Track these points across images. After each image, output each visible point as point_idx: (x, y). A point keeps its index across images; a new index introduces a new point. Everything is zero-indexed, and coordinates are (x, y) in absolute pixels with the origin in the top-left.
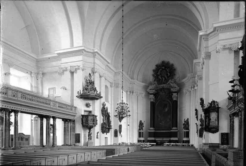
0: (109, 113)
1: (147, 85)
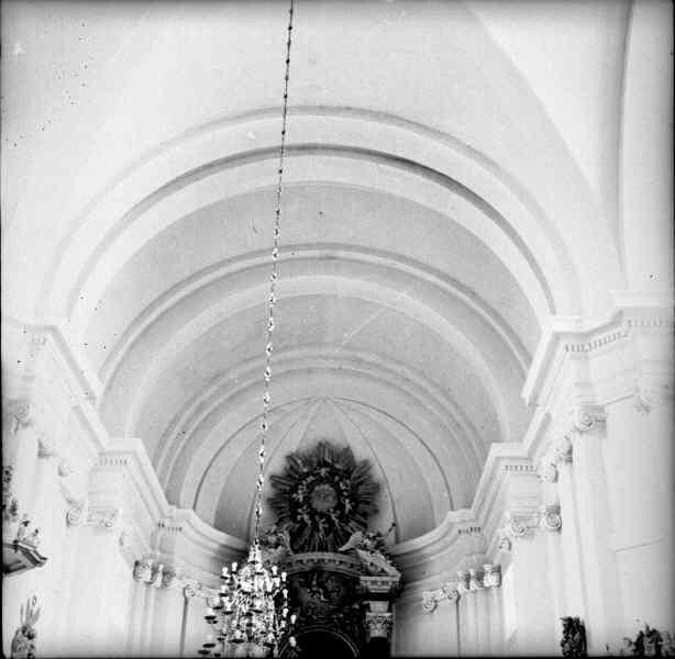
1: (237, 543)
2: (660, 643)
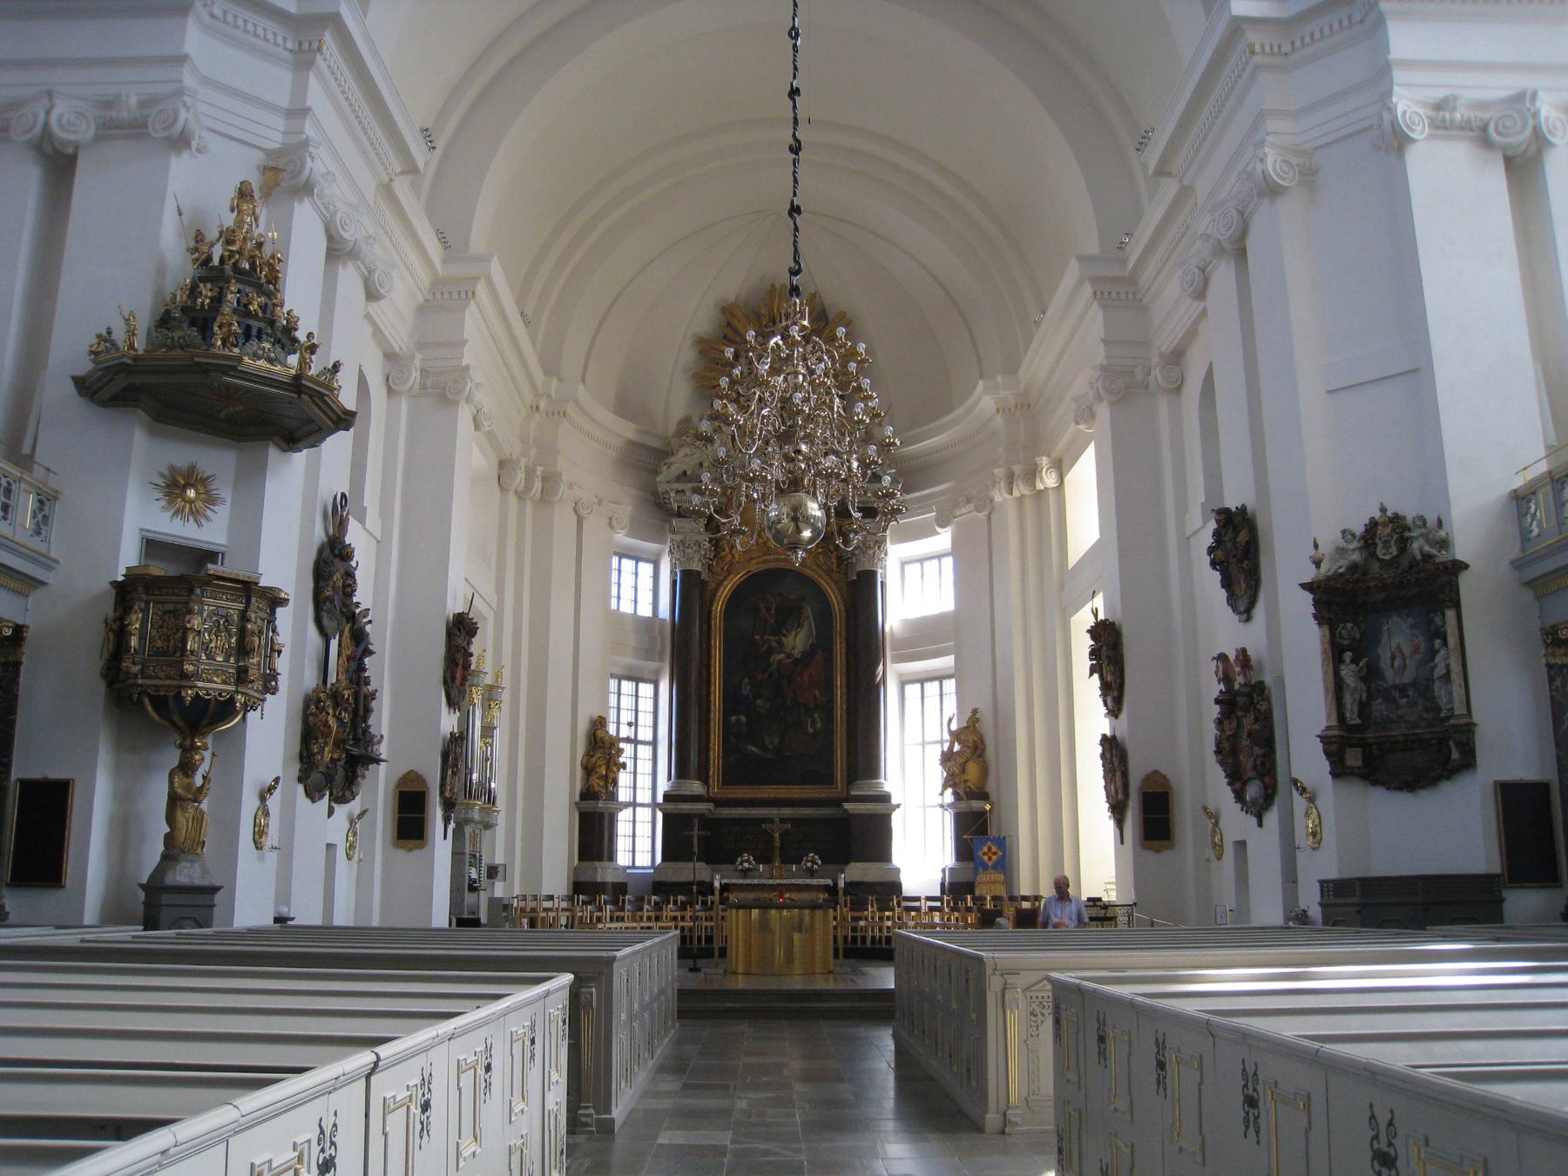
2: (1407, 534)
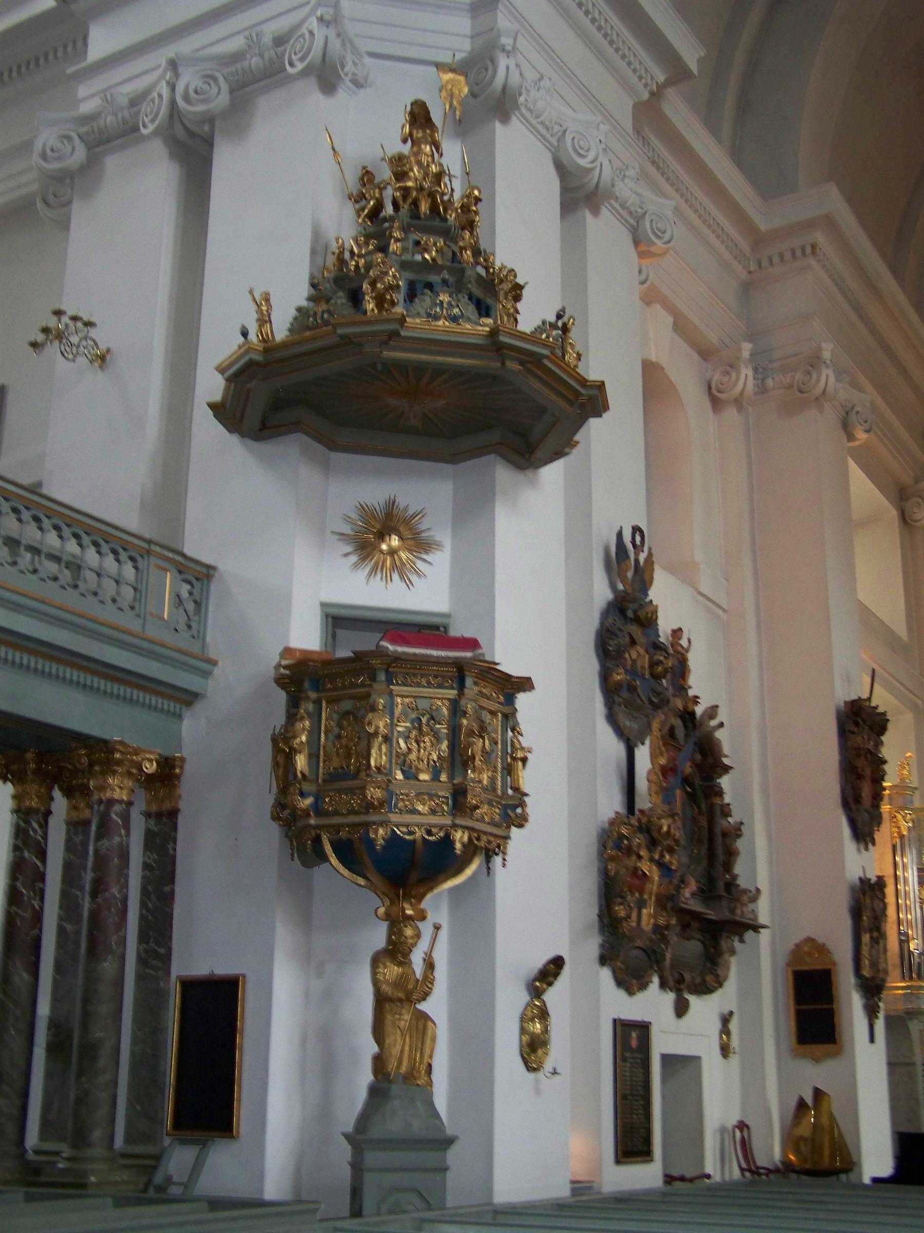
0: (712, 711)
